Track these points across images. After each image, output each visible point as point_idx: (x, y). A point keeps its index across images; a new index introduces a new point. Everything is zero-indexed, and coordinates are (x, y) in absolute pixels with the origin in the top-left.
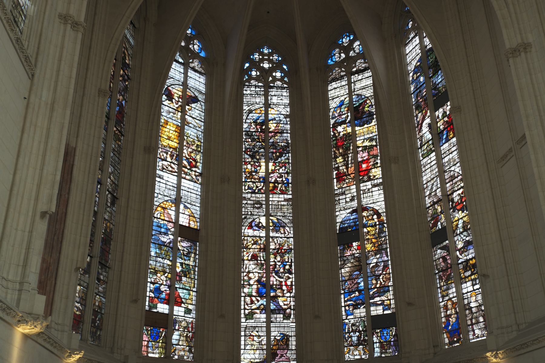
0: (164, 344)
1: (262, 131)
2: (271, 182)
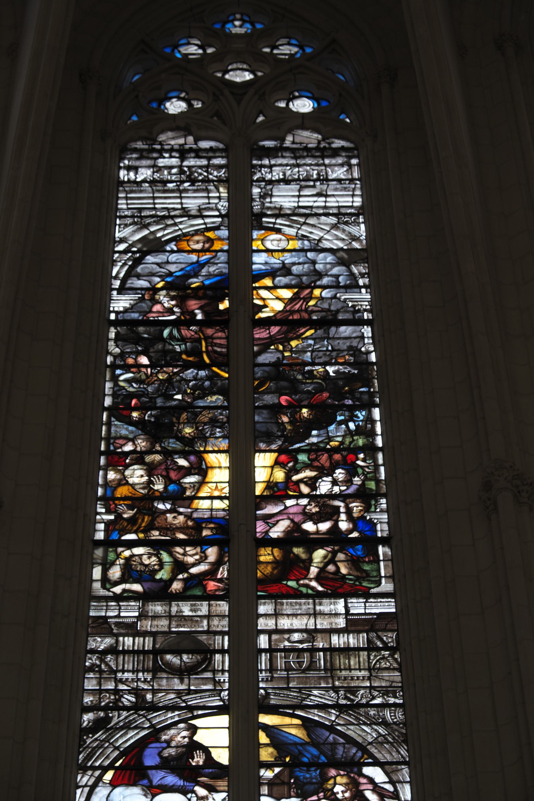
1: (214, 318)
2: (267, 542)
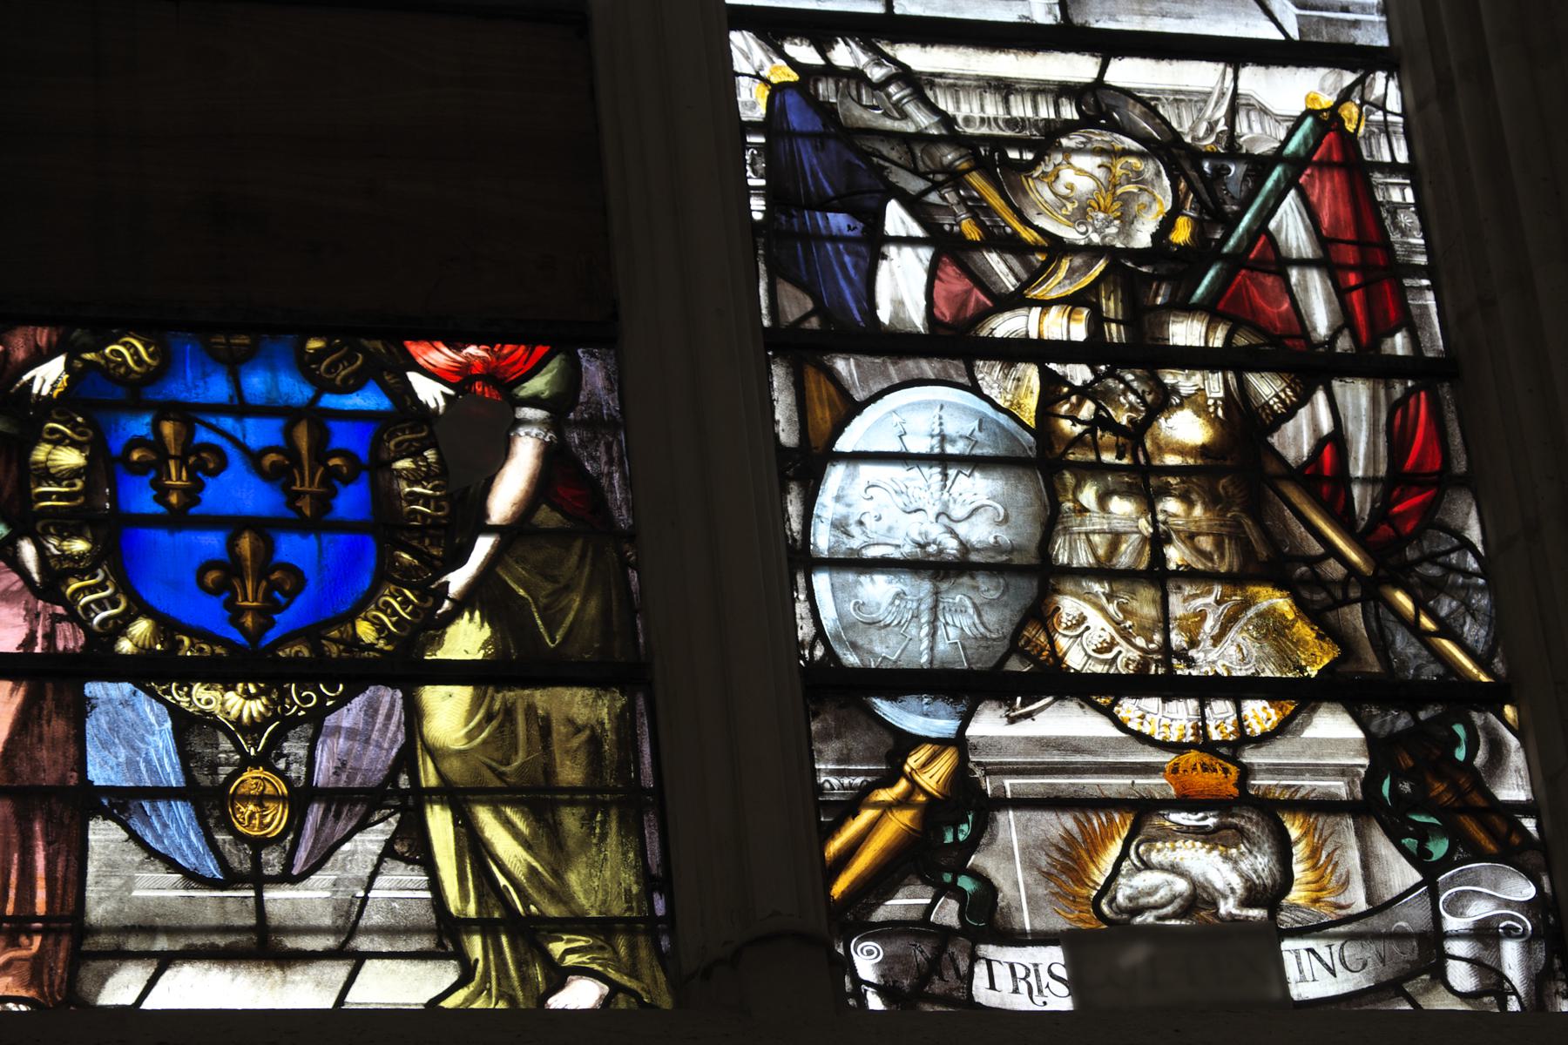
0: (578, 705)
